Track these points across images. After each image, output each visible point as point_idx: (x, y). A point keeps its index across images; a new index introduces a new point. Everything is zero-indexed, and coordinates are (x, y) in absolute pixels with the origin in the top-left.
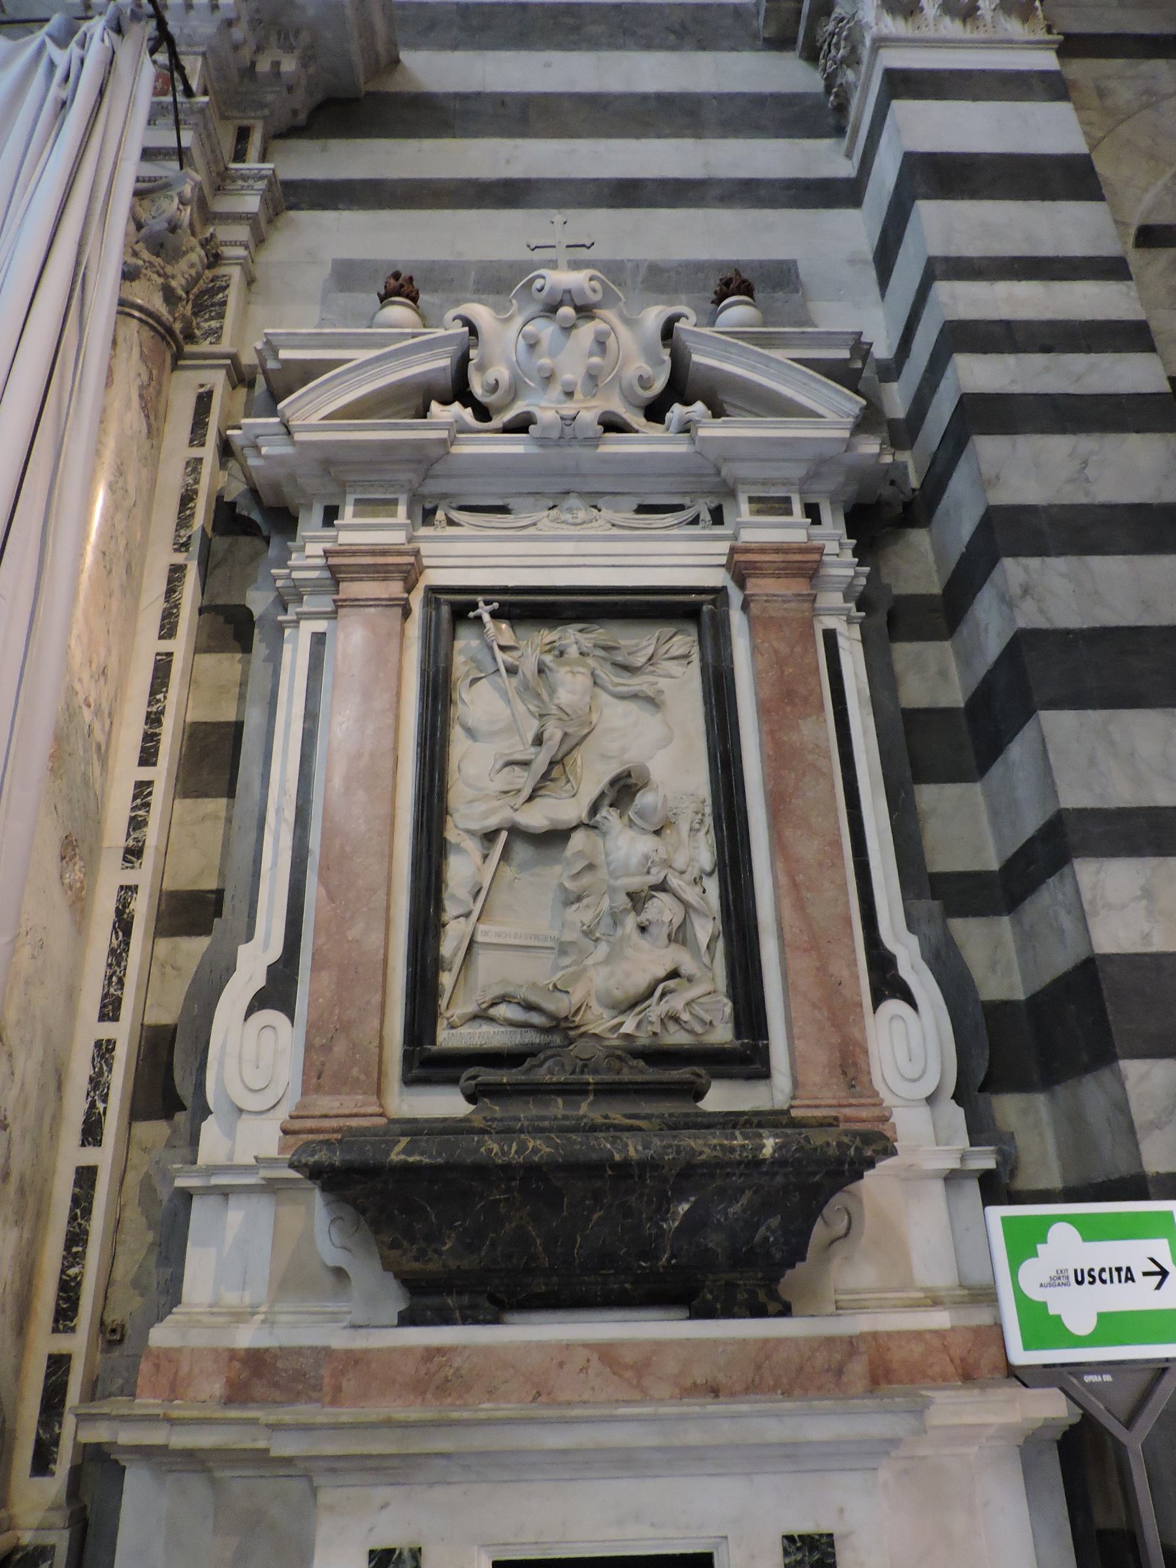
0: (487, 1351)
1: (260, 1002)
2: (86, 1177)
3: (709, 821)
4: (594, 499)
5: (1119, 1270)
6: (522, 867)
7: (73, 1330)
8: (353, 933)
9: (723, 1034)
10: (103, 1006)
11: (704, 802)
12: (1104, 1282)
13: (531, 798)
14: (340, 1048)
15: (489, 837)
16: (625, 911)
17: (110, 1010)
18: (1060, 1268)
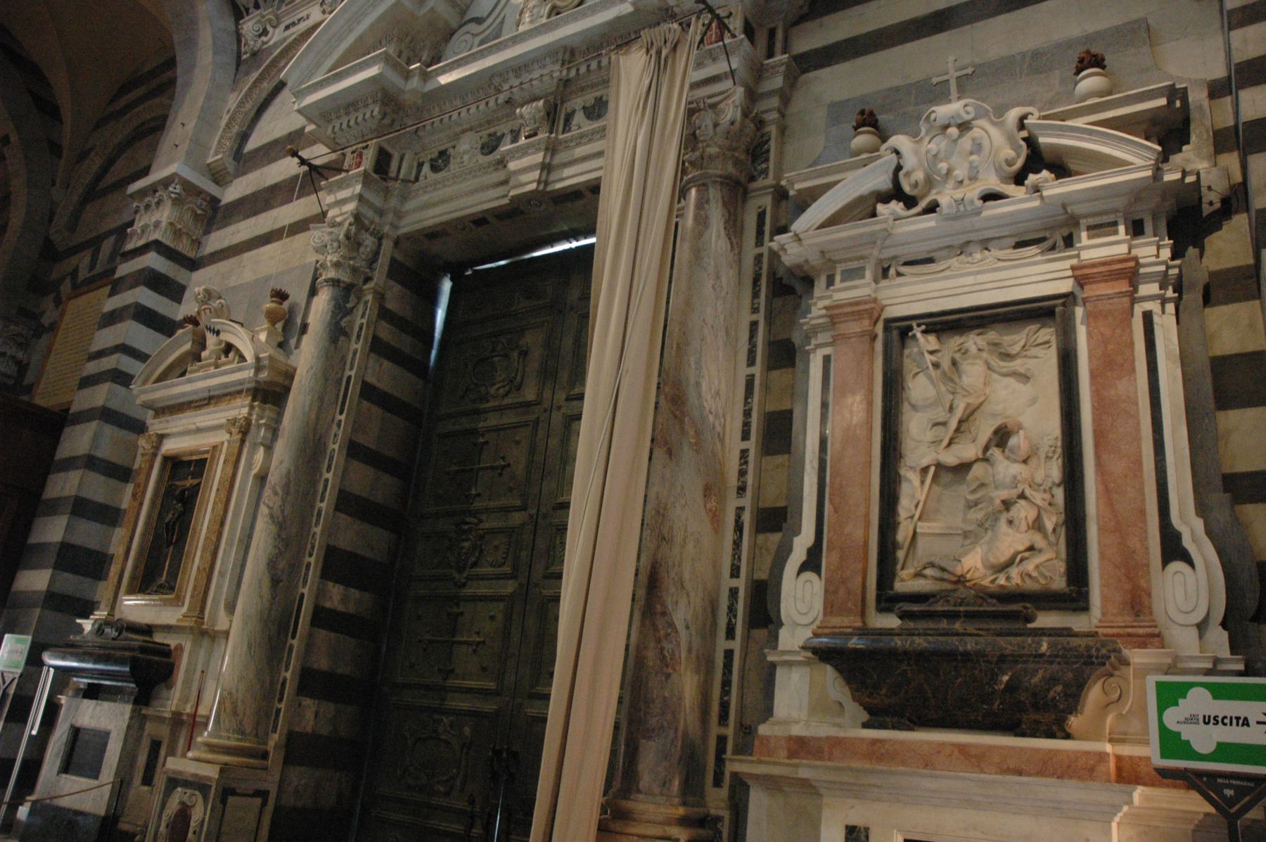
0: (902, 743)
1: (804, 568)
2: (729, 654)
3: (1059, 450)
4: (985, 244)
5: (1238, 719)
6: (946, 486)
7: (727, 725)
8: (848, 529)
9: (1059, 584)
10: (732, 570)
11: (1056, 439)
12: (1225, 724)
13: (949, 444)
14: (842, 592)
15: (925, 470)
16: (1000, 512)
17: (735, 573)
18: (1193, 713)
